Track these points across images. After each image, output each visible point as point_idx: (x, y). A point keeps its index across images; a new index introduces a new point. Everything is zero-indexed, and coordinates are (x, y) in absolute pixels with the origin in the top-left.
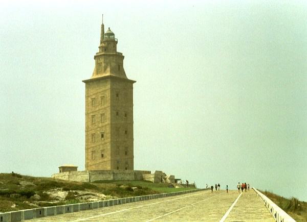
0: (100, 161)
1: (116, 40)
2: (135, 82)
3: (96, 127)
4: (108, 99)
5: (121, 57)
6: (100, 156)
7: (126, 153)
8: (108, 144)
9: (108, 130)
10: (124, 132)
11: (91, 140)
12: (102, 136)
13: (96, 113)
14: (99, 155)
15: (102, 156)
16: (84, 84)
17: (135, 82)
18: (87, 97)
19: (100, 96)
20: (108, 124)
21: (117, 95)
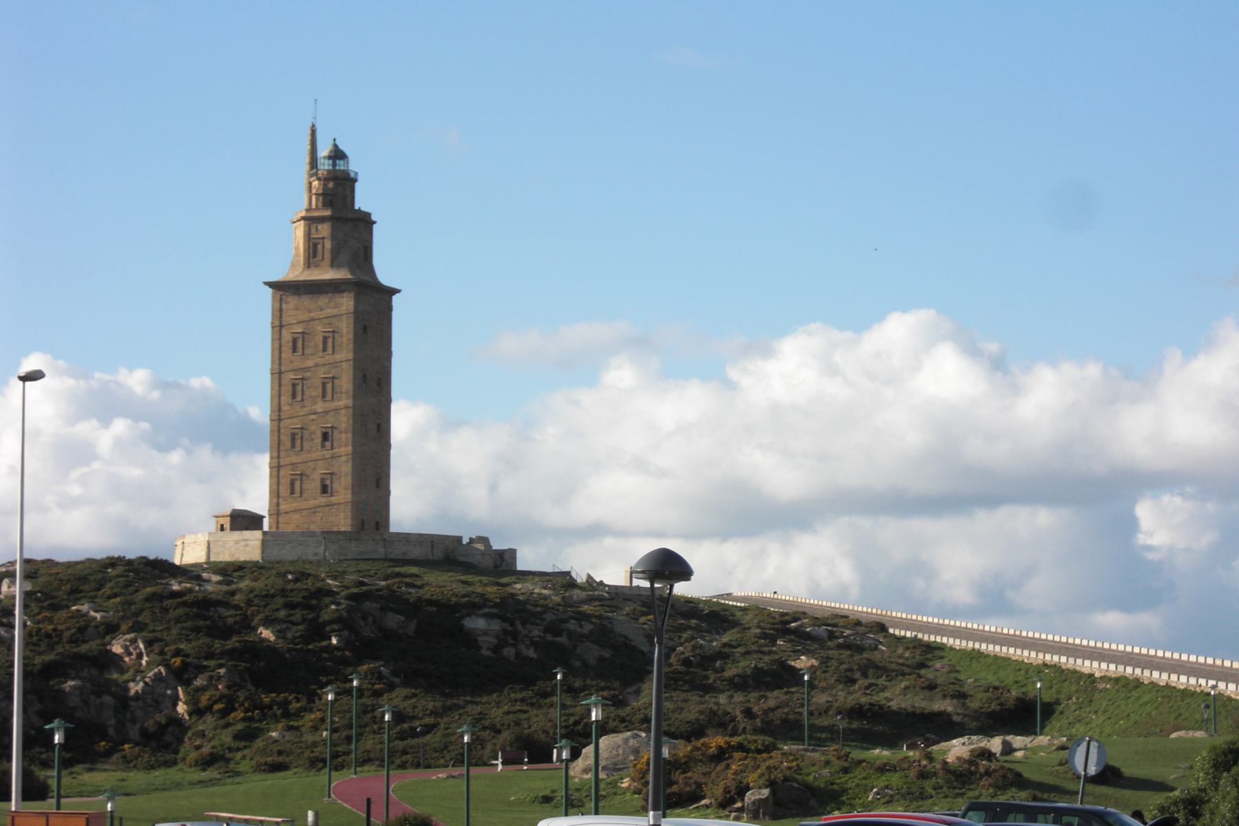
0: (317, 502)
1: (352, 175)
2: (398, 291)
3: (307, 410)
4: (345, 339)
5: (366, 221)
6: (319, 489)
7: (378, 485)
8: (344, 459)
9: (344, 421)
10: (375, 427)
11: (289, 445)
12: (325, 437)
13: (308, 374)
14: (314, 485)
15: (325, 489)
16: (269, 291)
17: (398, 291)
18: (279, 326)
19: (320, 328)
20: (346, 407)
21: (365, 328)
